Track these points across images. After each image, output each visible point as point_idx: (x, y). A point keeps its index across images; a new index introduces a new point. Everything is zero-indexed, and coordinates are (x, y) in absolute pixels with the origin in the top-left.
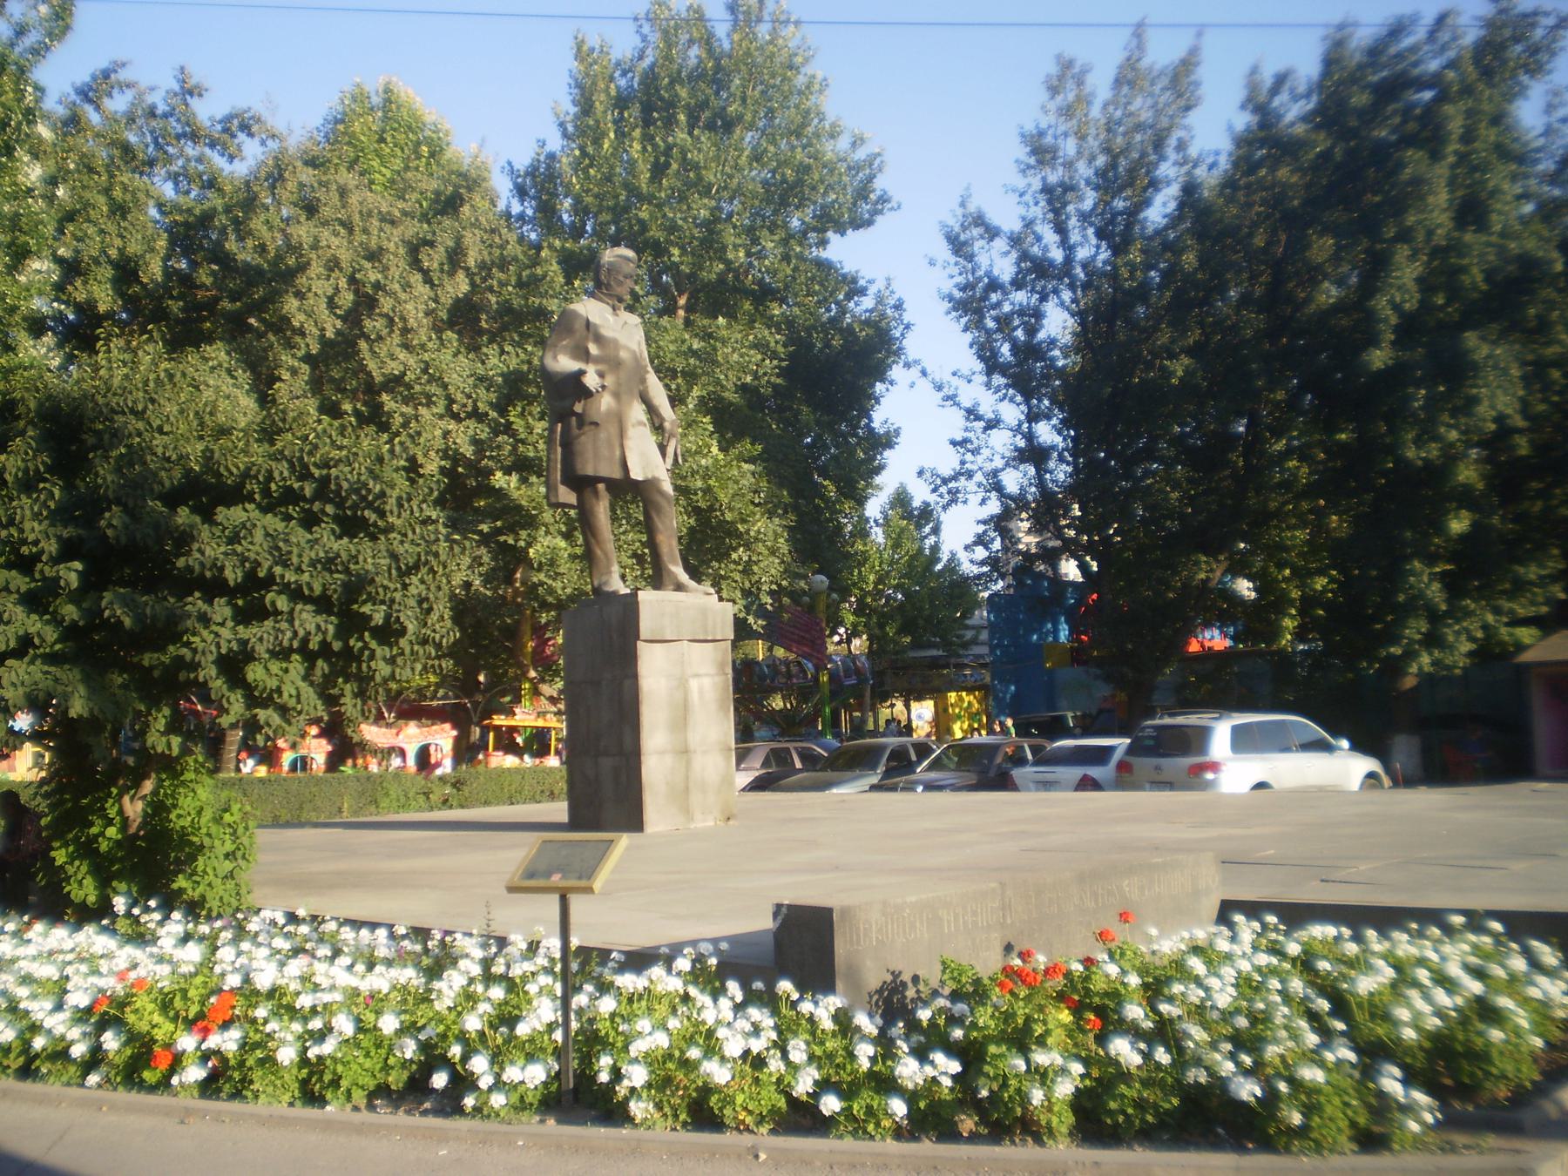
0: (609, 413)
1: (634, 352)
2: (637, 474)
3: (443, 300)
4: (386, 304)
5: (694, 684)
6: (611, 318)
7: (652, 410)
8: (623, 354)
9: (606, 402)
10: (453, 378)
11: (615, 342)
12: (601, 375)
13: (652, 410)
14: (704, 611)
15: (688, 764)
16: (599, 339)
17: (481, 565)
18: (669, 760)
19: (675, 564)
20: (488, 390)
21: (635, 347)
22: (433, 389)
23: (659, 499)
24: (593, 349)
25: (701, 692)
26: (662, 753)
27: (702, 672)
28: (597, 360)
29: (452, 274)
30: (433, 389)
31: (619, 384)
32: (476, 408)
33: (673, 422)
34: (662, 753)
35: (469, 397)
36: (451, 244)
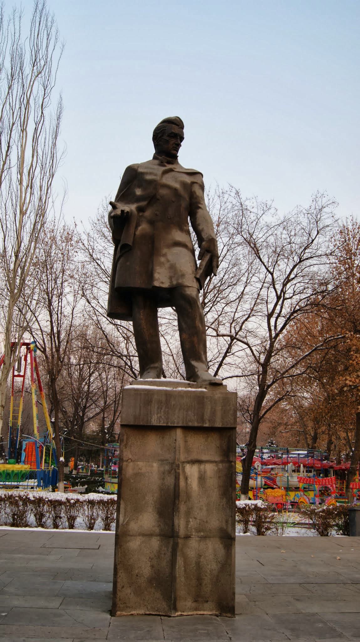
0: (144, 236)
1: (176, 190)
5: (192, 471)
8: (163, 192)
12: (140, 210)
18: (155, 543)
25: (202, 478)
26: (150, 535)
27: (204, 458)
28: (138, 199)
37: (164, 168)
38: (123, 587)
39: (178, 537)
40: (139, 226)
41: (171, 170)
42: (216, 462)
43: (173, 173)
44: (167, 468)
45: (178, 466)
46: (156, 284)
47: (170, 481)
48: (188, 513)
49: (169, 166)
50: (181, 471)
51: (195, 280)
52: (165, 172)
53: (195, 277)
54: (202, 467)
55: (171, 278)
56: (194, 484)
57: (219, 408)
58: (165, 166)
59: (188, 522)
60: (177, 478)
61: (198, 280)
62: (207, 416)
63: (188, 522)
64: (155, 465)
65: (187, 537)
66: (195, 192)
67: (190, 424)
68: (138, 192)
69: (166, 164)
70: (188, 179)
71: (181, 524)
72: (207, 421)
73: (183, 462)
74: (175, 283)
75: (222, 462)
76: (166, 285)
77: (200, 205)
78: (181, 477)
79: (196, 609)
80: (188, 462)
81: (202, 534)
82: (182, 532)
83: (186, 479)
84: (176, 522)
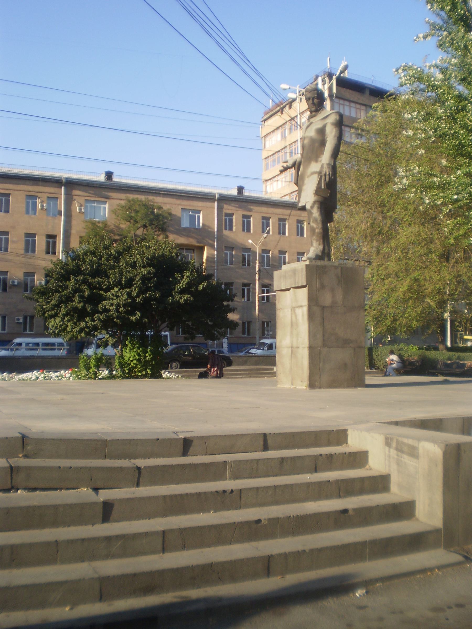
14: (294, 271)
25: (303, 315)
26: (289, 347)
38: (281, 373)
41: (311, 123)
43: (312, 125)
49: (312, 120)
51: (313, 195)
62: (297, 281)
65: (298, 348)
73: (294, 307)
77: (327, 139)
78: (293, 316)
79: (302, 386)
82: (295, 345)
83: (296, 316)
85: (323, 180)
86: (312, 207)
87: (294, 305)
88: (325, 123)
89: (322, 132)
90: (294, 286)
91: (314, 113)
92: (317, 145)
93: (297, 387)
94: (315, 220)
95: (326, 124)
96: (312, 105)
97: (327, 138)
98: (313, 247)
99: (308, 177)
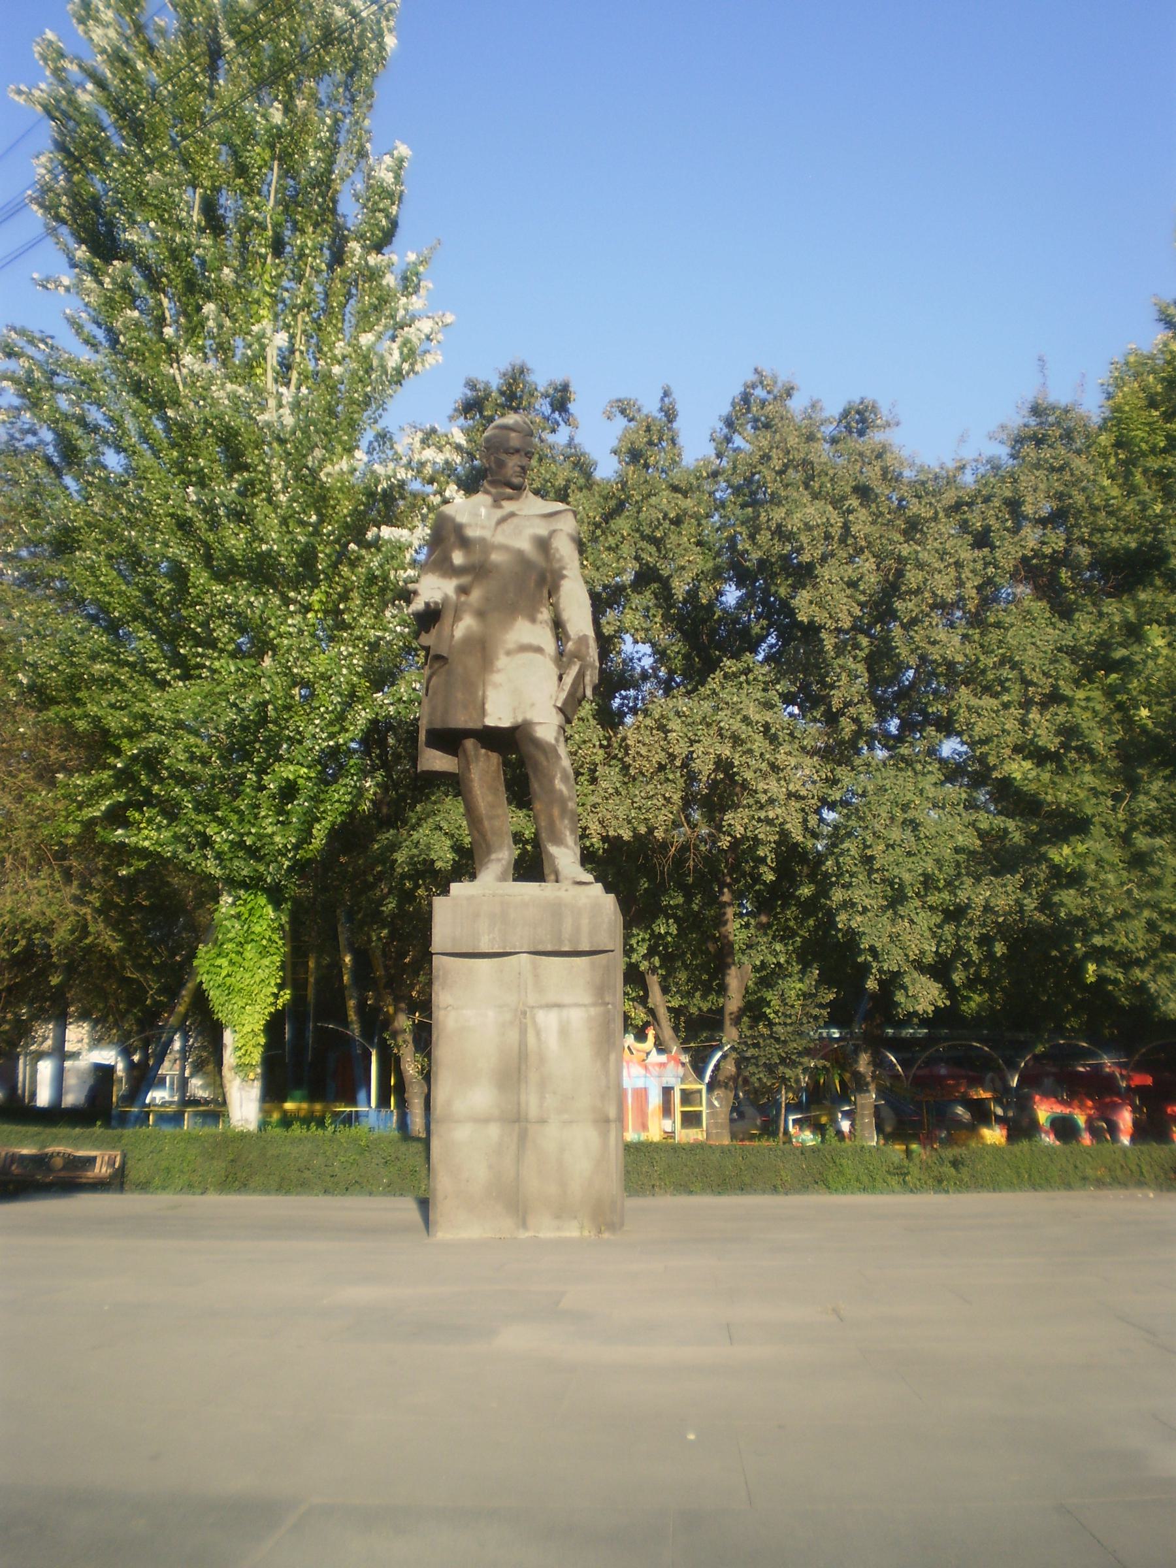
2: (498, 715)
3: (1002, 563)
4: (913, 577)
5: (548, 1021)
6: (483, 511)
7: (558, 625)
8: (496, 557)
9: (465, 626)
10: (1030, 657)
11: (486, 546)
12: (463, 590)
13: (558, 625)
14: (556, 910)
15: (523, 1137)
16: (465, 543)
17: (1038, 884)
18: (494, 1131)
19: (558, 841)
20: (1073, 662)
21: (524, 544)
22: (1006, 672)
23: (532, 750)
24: (458, 558)
25: (564, 1032)
26: (486, 1120)
27: (567, 1000)
29: (1016, 530)
30: (1006, 672)
31: (487, 599)
32: (1055, 687)
33: (583, 639)
34: (486, 1120)
35: (1046, 674)
36: (1008, 494)
37: (499, 513)
38: (446, 1197)
39: (527, 1121)
40: (460, 619)
41: (512, 515)
42: (585, 1006)
43: (515, 520)
44: (508, 1016)
45: (524, 1013)
46: (490, 721)
47: (513, 1036)
48: (543, 1084)
49: (509, 506)
50: (528, 1021)
51: (554, 711)
52: (502, 520)
53: (555, 706)
54: (565, 1012)
55: (514, 709)
56: (552, 1041)
57: (585, 922)
58: (500, 507)
59: (542, 1098)
60: (523, 1032)
61: (561, 710)
63: (542, 1098)
64: (491, 1014)
65: (543, 1121)
66: (557, 550)
67: (541, 948)
68: (458, 558)
69: (505, 503)
70: (542, 530)
71: (532, 1103)
72: (567, 942)
74: (520, 720)
75: (594, 1004)
76: (506, 723)
77: (565, 572)
79: (559, 1229)
80: (541, 1007)
81: (566, 1117)
82: (533, 1111)
83: (538, 1033)
84: (523, 1098)
85: (588, 679)
86: (557, 740)
87: (531, 1001)
88: (552, 528)
89: (543, 544)
90: (549, 948)
91: (509, 491)
92: (534, 577)
93: (541, 1235)
94: (565, 778)
95: (554, 531)
96: (518, 469)
97: (564, 568)
98: (567, 846)
99: (508, 653)
